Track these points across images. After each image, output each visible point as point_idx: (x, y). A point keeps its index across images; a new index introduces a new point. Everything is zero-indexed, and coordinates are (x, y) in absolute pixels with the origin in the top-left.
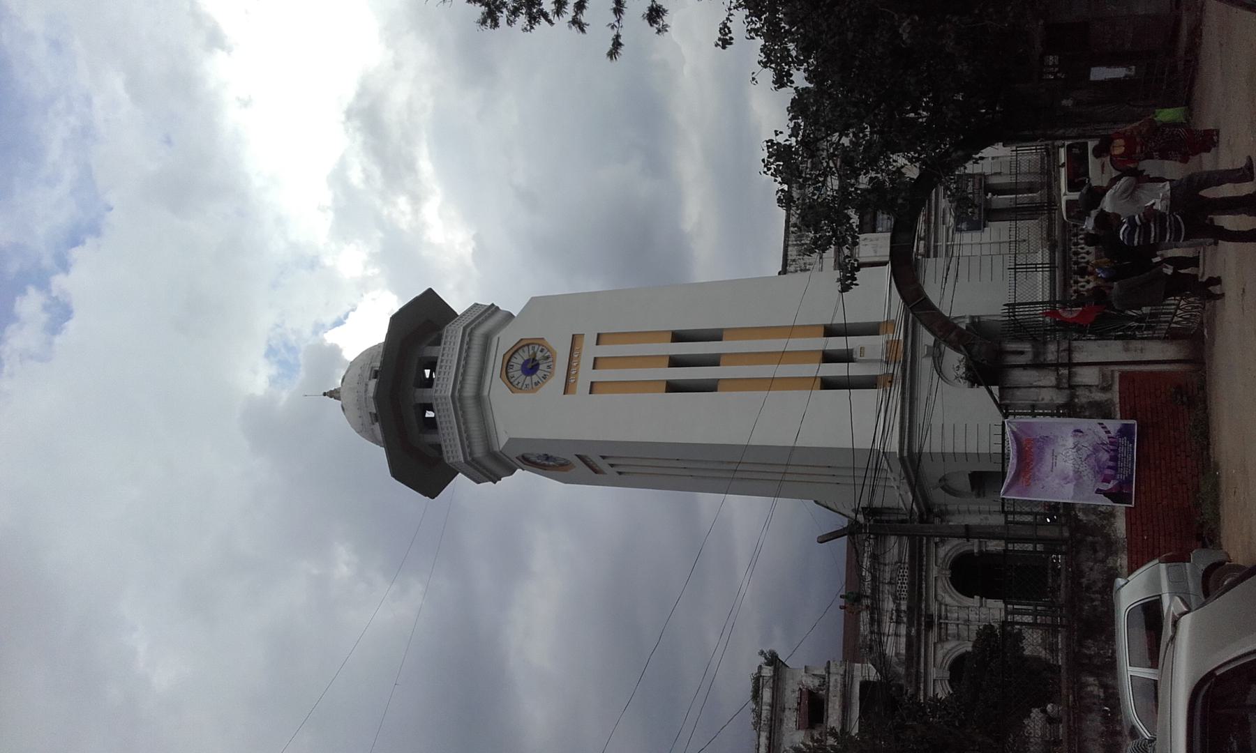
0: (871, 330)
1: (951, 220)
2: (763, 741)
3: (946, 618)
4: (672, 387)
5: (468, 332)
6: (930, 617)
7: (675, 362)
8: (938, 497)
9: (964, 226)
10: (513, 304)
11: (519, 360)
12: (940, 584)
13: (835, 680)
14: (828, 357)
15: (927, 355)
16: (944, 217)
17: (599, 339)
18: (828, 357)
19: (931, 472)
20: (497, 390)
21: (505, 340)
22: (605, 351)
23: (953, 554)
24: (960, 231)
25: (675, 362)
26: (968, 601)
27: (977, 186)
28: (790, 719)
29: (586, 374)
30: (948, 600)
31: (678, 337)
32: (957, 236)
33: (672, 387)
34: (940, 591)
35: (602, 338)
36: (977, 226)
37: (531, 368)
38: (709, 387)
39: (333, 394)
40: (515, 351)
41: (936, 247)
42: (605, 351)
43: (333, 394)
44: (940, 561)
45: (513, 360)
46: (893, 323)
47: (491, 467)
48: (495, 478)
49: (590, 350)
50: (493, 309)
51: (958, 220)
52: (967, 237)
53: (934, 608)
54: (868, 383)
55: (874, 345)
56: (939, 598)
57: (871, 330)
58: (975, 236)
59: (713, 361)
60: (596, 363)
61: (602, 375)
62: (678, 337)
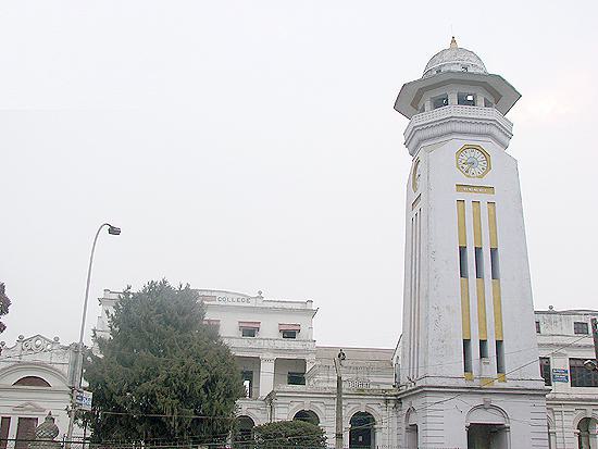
0: (500, 369)
4: (462, 250)
5: (492, 123)
7: (478, 251)
8: (405, 405)
10: (514, 148)
13: (310, 346)
14: (483, 343)
18: (483, 343)
19: (417, 403)
20: (458, 143)
21: (489, 146)
22: (484, 207)
25: (478, 251)
29: (469, 197)
31: (494, 252)
33: (462, 250)
35: (491, 206)
38: (463, 273)
39: (454, 41)
40: (483, 152)
42: (484, 207)
43: (454, 41)
47: (414, 142)
48: (407, 144)
49: (483, 198)
50: (510, 136)
54: (467, 369)
55: (490, 370)
57: (500, 369)
59: (479, 275)
61: (469, 206)
62: (494, 252)
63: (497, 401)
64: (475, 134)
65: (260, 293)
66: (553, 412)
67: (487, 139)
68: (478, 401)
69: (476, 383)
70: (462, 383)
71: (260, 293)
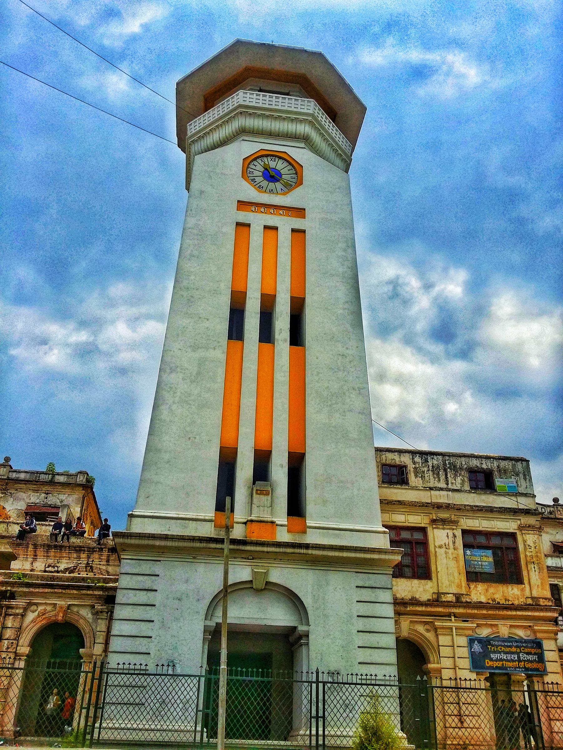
0: (296, 507)
1: (484, 632)
2: (22, 476)
3: (7, 615)
6: (13, 596)
9: (477, 647)
11: (280, 165)
12: (49, 608)
15: (254, 573)
16: (486, 625)
17: (298, 233)
20: (248, 147)
22: (284, 237)
23: (82, 624)
24: (471, 641)
26: (26, 638)
27: (528, 665)
28: (35, 498)
29: (258, 221)
30: (31, 616)
32: (462, 641)
34: (41, 608)
36: (477, 664)
37: (272, 176)
38: (236, 330)
41: (449, 615)
44: (75, 609)
45: (281, 161)
46: (305, 532)
49: (285, 224)
51: (485, 642)
52: (464, 652)
53: (20, 602)
56: (33, 608)
57: (296, 507)
58: (466, 663)
60: (270, 229)
61: (256, 236)
63: (279, 574)
64: (270, 134)
65: (7, 459)
66: (436, 629)
67: (303, 145)
68: (241, 572)
69: (238, 532)
70: (208, 531)
71: (7, 459)
